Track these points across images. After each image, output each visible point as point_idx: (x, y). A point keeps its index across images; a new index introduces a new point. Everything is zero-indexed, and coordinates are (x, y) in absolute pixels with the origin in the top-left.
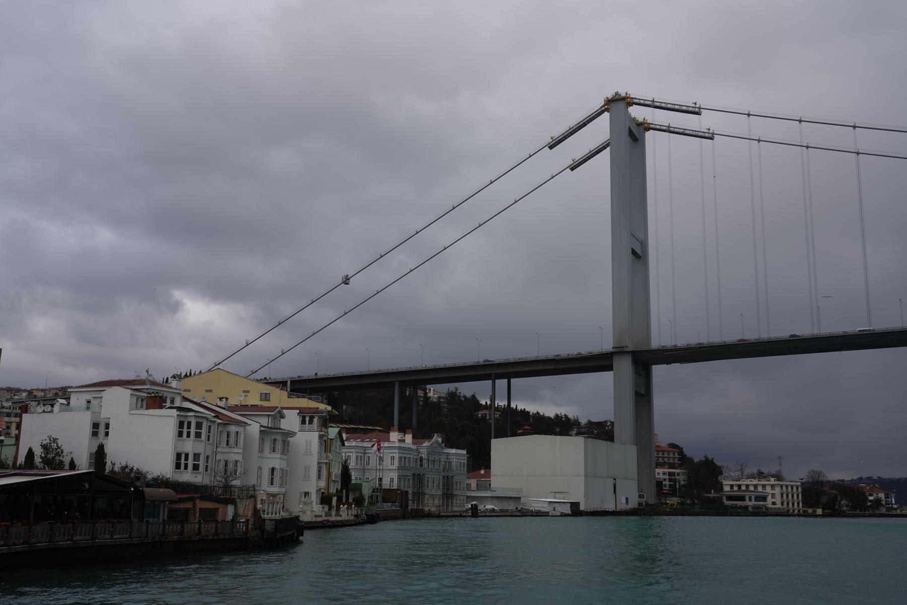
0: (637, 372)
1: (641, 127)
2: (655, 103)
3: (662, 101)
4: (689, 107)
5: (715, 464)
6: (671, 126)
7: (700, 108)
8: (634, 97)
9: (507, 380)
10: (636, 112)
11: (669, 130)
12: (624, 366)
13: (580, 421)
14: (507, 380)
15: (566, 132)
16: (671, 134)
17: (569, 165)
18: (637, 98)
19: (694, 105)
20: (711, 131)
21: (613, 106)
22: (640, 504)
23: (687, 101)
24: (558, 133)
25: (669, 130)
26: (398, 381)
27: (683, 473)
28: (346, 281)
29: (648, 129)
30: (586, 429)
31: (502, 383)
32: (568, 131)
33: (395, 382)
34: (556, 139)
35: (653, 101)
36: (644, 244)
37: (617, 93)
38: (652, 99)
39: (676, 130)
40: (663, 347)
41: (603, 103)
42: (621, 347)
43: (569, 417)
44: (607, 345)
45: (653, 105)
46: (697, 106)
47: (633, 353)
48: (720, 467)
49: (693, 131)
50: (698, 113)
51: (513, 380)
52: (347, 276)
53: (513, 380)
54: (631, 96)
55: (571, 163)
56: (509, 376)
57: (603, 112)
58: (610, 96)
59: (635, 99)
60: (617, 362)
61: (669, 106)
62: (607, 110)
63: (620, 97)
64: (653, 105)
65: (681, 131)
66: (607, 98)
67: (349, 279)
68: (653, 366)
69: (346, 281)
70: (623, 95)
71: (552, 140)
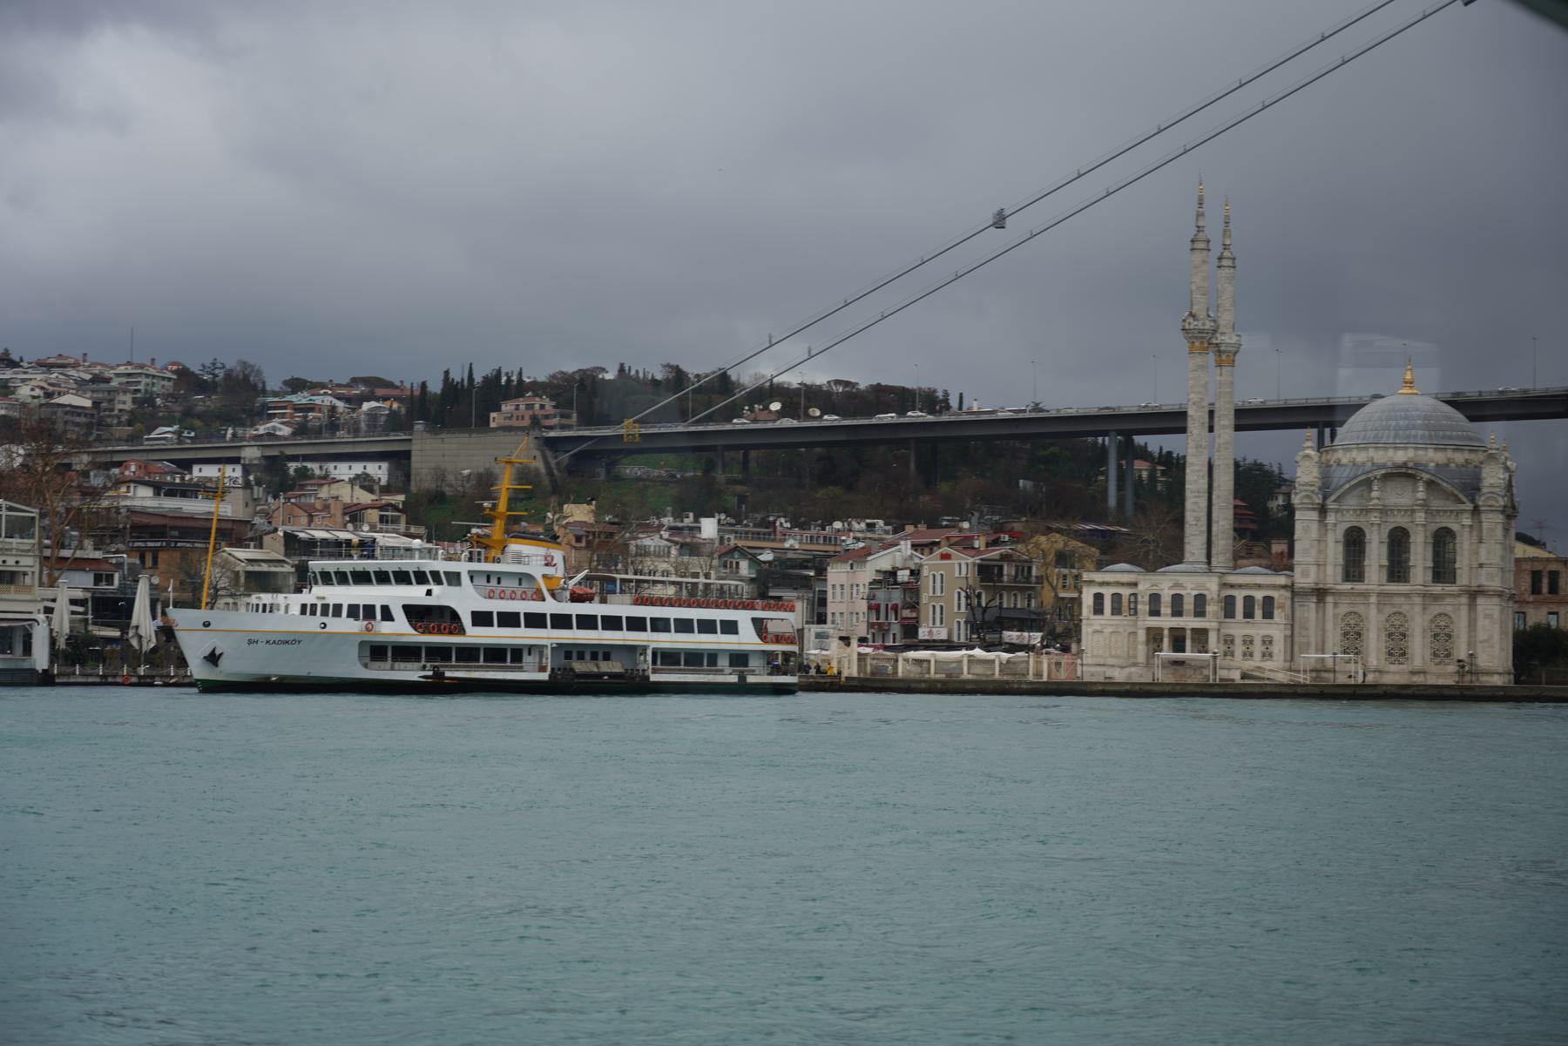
28: (1000, 221)
69: (1000, 221)
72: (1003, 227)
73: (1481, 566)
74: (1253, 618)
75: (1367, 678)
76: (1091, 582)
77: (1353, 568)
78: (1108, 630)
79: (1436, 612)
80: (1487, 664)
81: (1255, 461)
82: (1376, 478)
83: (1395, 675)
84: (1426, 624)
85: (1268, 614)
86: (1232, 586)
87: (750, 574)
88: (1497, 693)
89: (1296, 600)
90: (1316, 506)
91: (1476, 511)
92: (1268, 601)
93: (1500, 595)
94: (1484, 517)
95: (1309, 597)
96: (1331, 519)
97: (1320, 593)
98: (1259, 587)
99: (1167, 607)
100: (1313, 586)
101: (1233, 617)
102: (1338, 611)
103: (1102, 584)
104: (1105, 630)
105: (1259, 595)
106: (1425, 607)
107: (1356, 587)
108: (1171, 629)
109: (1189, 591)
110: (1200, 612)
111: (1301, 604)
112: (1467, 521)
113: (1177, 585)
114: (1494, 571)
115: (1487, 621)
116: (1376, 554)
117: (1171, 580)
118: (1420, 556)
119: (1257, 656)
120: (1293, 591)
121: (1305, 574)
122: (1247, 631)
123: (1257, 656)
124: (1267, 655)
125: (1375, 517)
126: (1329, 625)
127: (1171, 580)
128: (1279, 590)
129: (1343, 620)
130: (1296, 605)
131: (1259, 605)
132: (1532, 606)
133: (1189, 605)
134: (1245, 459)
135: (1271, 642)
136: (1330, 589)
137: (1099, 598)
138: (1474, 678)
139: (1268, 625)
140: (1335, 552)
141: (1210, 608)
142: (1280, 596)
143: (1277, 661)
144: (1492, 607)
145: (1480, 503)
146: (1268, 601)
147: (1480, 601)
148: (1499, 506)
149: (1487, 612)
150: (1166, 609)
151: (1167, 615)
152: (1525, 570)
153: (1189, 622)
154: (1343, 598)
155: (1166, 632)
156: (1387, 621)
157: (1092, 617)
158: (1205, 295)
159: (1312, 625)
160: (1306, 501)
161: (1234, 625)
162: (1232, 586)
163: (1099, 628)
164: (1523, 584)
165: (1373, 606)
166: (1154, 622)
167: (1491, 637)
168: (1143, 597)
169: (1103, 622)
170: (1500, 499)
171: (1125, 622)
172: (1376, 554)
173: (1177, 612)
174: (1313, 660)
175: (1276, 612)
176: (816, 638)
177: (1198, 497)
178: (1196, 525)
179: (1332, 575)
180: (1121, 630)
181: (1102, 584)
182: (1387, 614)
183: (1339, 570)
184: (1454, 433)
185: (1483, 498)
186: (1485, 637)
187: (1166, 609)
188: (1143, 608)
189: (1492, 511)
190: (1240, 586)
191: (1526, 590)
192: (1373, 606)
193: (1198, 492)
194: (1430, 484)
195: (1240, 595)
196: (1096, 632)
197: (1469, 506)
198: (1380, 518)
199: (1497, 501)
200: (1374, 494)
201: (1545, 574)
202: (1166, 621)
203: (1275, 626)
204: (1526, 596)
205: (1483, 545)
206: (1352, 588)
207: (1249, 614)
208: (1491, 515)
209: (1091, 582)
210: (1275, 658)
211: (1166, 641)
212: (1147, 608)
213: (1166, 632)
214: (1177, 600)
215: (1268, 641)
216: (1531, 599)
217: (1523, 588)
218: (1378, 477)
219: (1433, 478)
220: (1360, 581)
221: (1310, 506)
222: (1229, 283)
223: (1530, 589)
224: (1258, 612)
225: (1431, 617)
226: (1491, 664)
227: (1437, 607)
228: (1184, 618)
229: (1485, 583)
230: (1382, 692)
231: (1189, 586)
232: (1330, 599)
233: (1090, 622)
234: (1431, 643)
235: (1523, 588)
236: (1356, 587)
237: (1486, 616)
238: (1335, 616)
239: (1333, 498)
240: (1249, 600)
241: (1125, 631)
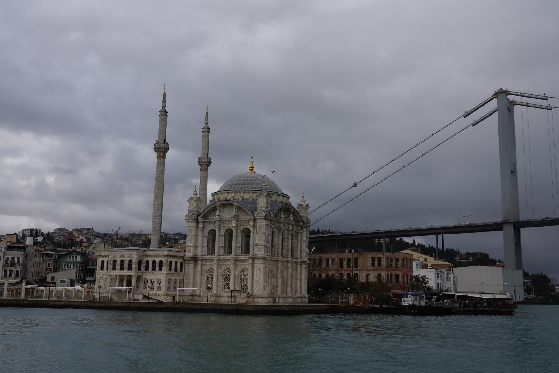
0: (515, 232)
1: (511, 104)
2: (522, 94)
3: (526, 93)
4: (541, 96)
5: (547, 277)
6: (528, 103)
7: (547, 97)
8: (510, 91)
9: (441, 235)
10: (510, 97)
11: (527, 105)
12: (509, 229)
13: (460, 252)
14: (441, 235)
15: (473, 109)
16: (528, 107)
17: (471, 123)
18: (512, 91)
19: (544, 95)
20: (550, 106)
21: (499, 96)
22: (525, 299)
23: (540, 93)
24: (469, 109)
25: (527, 105)
26: (385, 236)
27: (529, 282)
28: (355, 185)
29: (515, 105)
30: (464, 257)
31: (440, 236)
32: (474, 108)
33: (383, 236)
34: (467, 113)
35: (521, 93)
36: (514, 165)
37: (501, 89)
38: (520, 92)
39: (531, 105)
40: (530, 220)
41: (494, 94)
42: (507, 220)
43: (454, 250)
44: (498, 219)
45: (521, 95)
46: (546, 95)
47: (514, 223)
48: (549, 279)
49: (541, 105)
50: (547, 100)
51: (444, 235)
52: (355, 183)
53: (444, 235)
54: (509, 90)
55: (473, 123)
56: (442, 234)
57: (493, 99)
58: (497, 91)
59: (511, 92)
60: (505, 227)
61: (530, 96)
62: (496, 98)
63: (503, 91)
64: (521, 95)
65: (534, 105)
66: (496, 91)
67: (356, 184)
68: (521, 228)
69: (355, 185)
70: (504, 90)
71: (465, 113)
72: (356, 187)
73: (256, 245)
74: (155, 271)
75: (211, 299)
76: (99, 256)
77: (211, 249)
79: (242, 268)
80: (258, 293)
81: (467, 252)
82: (218, 206)
83: (225, 299)
84: (237, 274)
85: (161, 269)
86: (147, 256)
87: (81, 260)
88: (217, 308)
89: (186, 263)
90: (193, 220)
91: (255, 220)
92: (161, 262)
93: (264, 259)
94: (257, 221)
95: (190, 261)
96: (201, 226)
97: (195, 259)
98: (157, 256)
99: (119, 266)
100: (191, 256)
101: (148, 270)
102: (204, 268)
104: (103, 277)
105: (157, 260)
106: (236, 265)
107: (212, 257)
108: (120, 276)
109: (126, 258)
110: (130, 268)
111: (187, 265)
112: (252, 224)
113: (122, 256)
114: (261, 247)
115: (258, 272)
116: (220, 241)
117: (121, 253)
118: (237, 242)
119: (155, 288)
120: (184, 259)
121: (189, 251)
122: (152, 277)
123: (155, 288)
124: (159, 288)
125: (217, 224)
126: (199, 274)
127: (121, 253)
128: (164, 257)
129: (207, 272)
130: (186, 265)
131: (157, 264)
132: (372, 271)
133: (126, 265)
134: (449, 248)
135: (161, 282)
136: (198, 258)
137: (103, 262)
138: (252, 299)
139: (160, 274)
140: (203, 241)
141: (134, 266)
142: (165, 260)
143: (162, 291)
144: (260, 265)
145: (256, 215)
146: (161, 262)
147: (256, 262)
148: (263, 216)
149: (258, 267)
150: (118, 267)
151: (118, 269)
152: (369, 257)
153: (126, 273)
154: (207, 262)
156: (224, 272)
157: (100, 271)
158: (162, 133)
159: (191, 274)
160: (190, 218)
161: (148, 274)
162: (147, 256)
163: (101, 276)
164: (369, 263)
165: (215, 265)
167: (260, 279)
168: (110, 261)
169: (103, 273)
170: (263, 213)
172: (220, 241)
173: (122, 269)
174: (191, 290)
175: (164, 268)
176: (60, 282)
177: (156, 218)
178: (154, 231)
179: (201, 252)
182: (223, 269)
183: (205, 249)
184: (257, 186)
185: (256, 213)
186: (257, 279)
187: (118, 267)
188: (110, 266)
189: (261, 218)
190: (151, 256)
191: (370, 265)
192: (215, 265)
193: (155, 216)
194: (239, 208)
195: (151, 260)
196: (101, 278)
197: (252, 217)
198: (219, 224)
199: (262, 214)
200: (217, 214)
201: (376, 258)
202: (118, 272)
204: (370, 267)
205: (257, 235)
206: (210, 257)
207: (154, 269)
208: (260, 221)
209: (99, 256)
210: (162, 289)
211: (125, 282)
212: (112, 266)
214: (122, 262)
215: (159, 281)
216: (371, 268)
217: (369, 264)
218: (219, 206)
219: (239, 205)
220: (213, 254)
221: (191, 220)
222: (206, 138)
223: (371, 265)
224: (157, 268)
225: (240, 270)
226: (259, 293)
227: (243, 266)
228: (124, 271)
229: (258, 253)
230: (166, 306)
231: (126, 256)
232: (199, 262)
233: (99, 273)
234: (206, 282)
235: (369, 264)
236: (212, 257)
237: (258, 269)
238: (202, 270)
239: (201, 216)
240: (154, 262)
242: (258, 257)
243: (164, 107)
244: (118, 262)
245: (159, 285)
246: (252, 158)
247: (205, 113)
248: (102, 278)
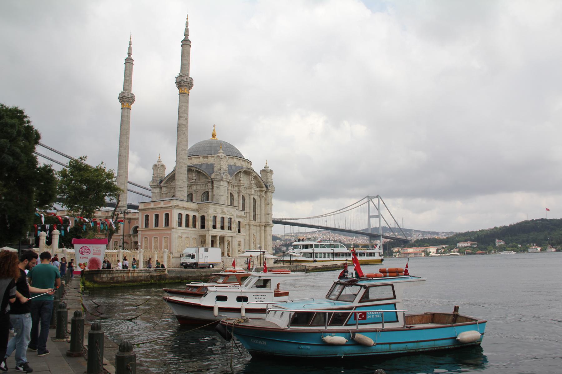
76: (177, 207)
78: (184, 236)
103: (184, 208)
104: (182, 236)
117: (221, 209)
127: (221, 209)
150: (219, 225)
155: (218, 238)
163: (180, 235)
166: (214, 232)
169: (182, 231)
171: (191, 232)
175: (242, 230)
180: (189, 236)
181: (184, 208)
187: (219, 225)
203: (242, 236)
209: (177, 207)
213: (218, 238)
218: (243, 172)
241: (191, 237)
242: (270, 225)
243: (186, 35)
244: (219, 220)
245: (239, 248)
246: (214, 126)
247: (128, 43)
248: (181, 237)
